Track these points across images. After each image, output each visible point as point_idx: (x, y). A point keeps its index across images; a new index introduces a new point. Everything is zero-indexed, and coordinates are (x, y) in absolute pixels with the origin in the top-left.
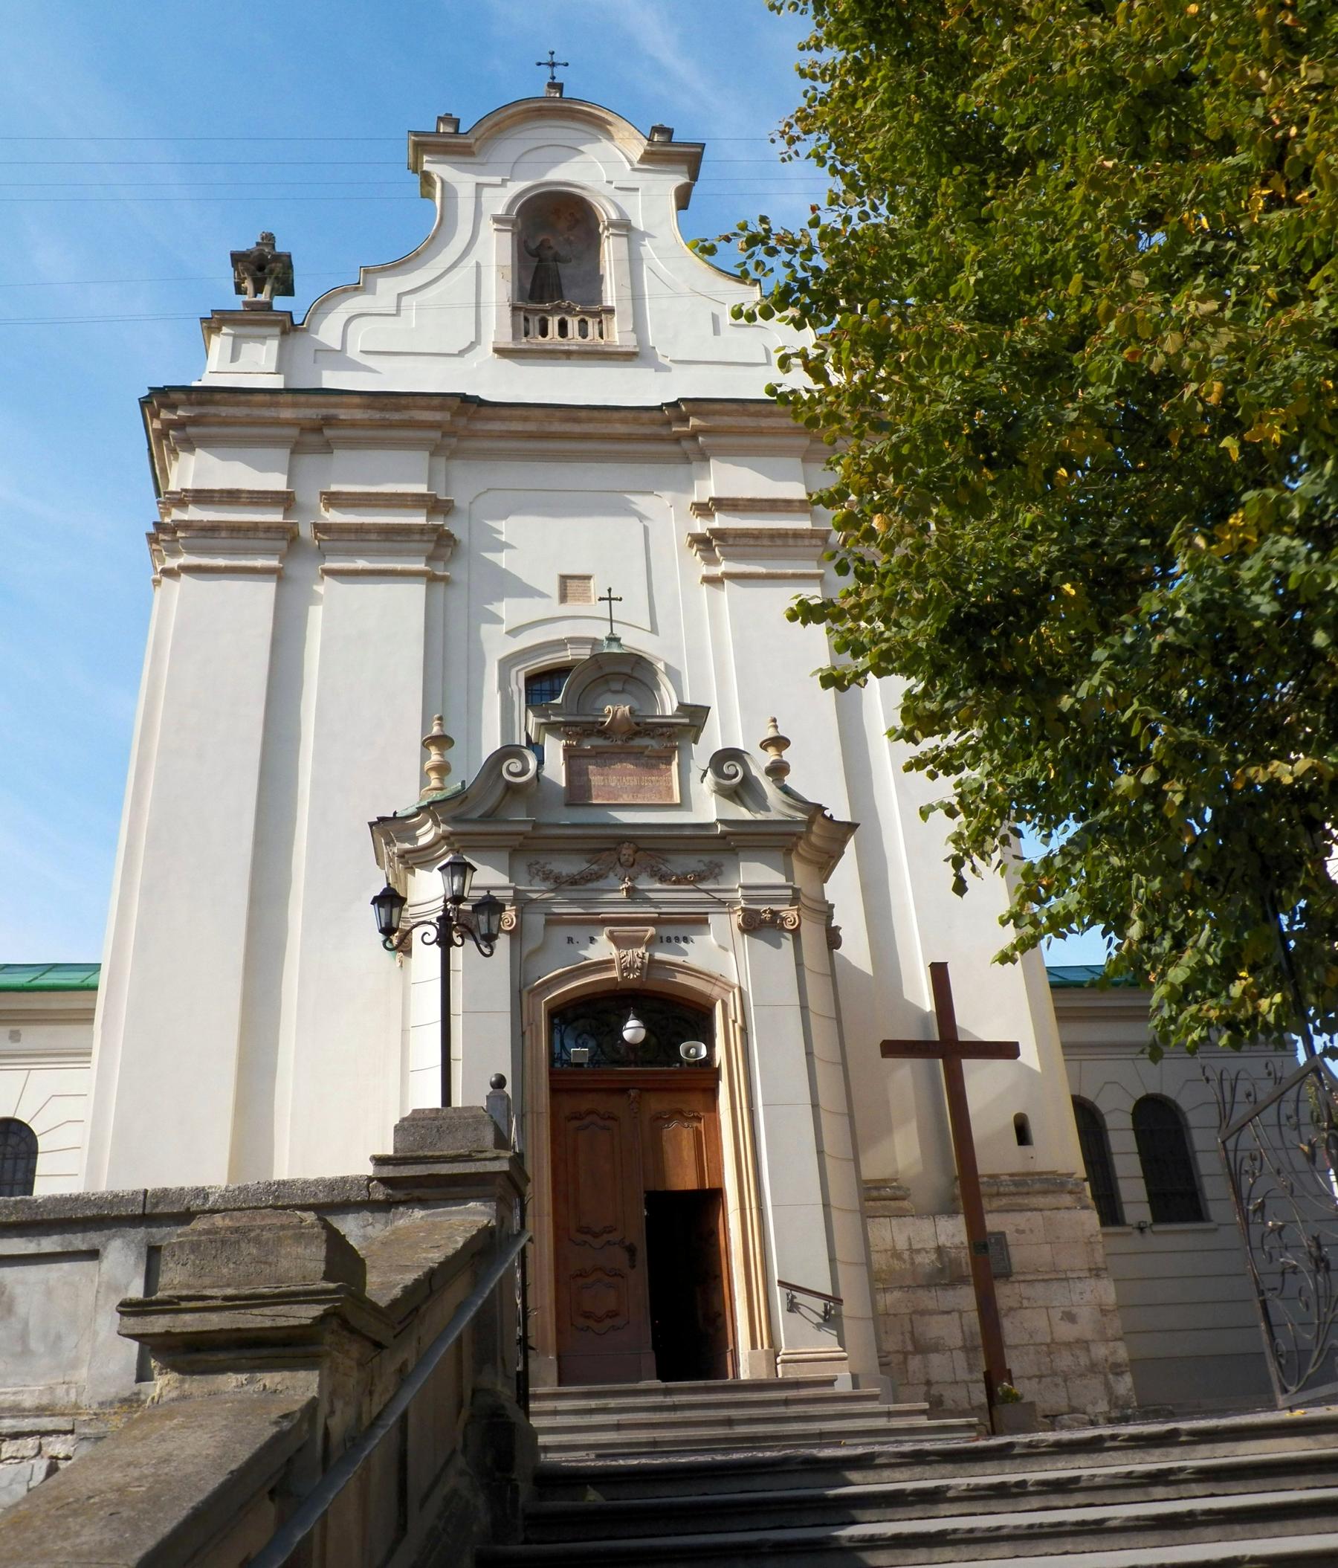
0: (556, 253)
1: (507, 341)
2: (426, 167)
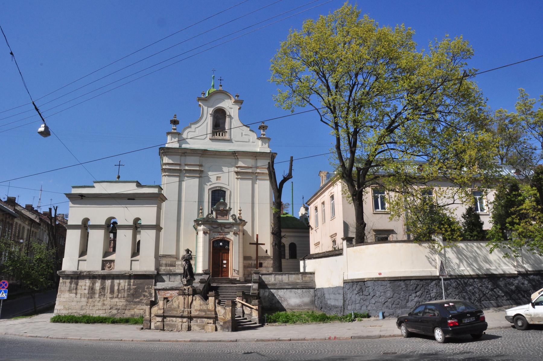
1: (211, 138)
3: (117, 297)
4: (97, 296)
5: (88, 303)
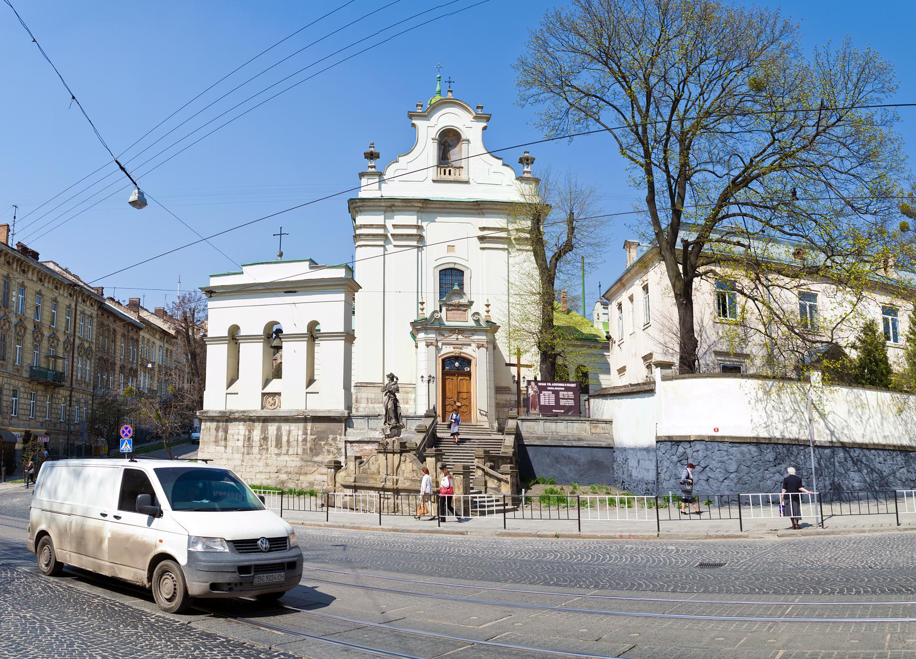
3: (287, 453)
4: (256, 450)
5: (243, 461)
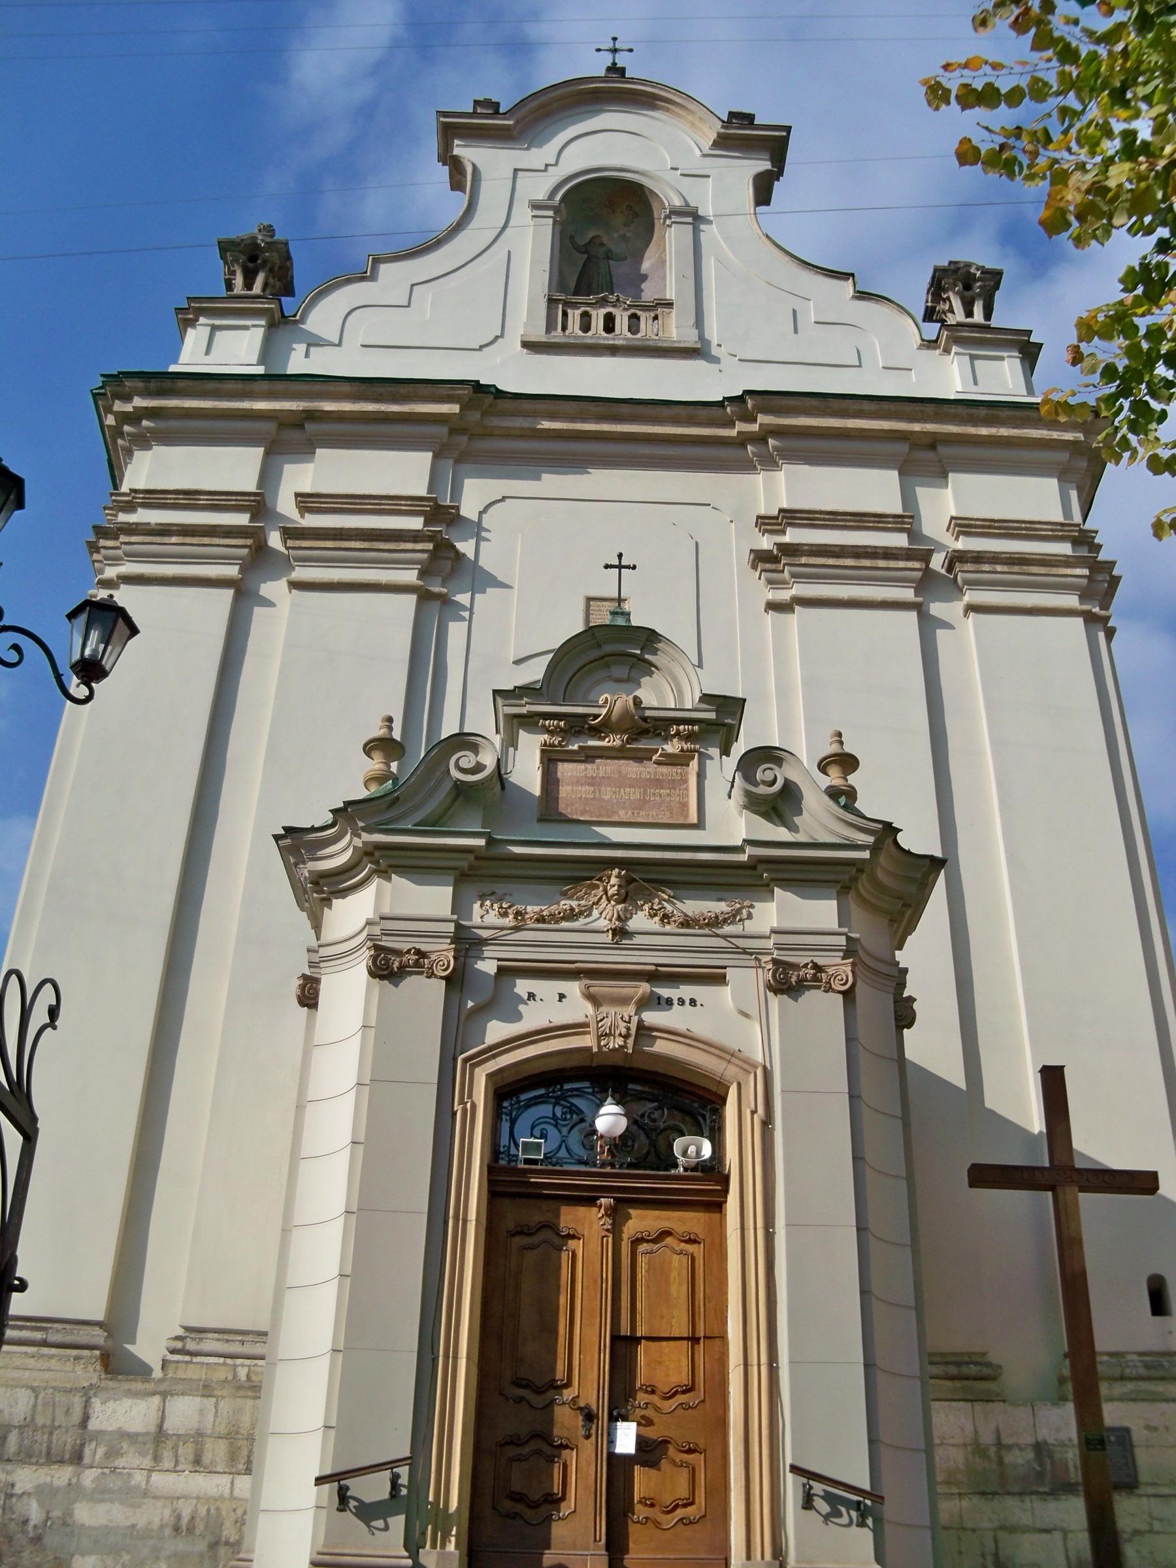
0: (610, 250)
1: (539, 334)
2: (457, 151)
